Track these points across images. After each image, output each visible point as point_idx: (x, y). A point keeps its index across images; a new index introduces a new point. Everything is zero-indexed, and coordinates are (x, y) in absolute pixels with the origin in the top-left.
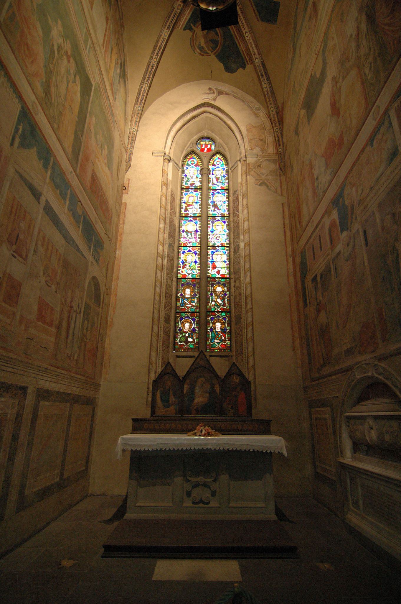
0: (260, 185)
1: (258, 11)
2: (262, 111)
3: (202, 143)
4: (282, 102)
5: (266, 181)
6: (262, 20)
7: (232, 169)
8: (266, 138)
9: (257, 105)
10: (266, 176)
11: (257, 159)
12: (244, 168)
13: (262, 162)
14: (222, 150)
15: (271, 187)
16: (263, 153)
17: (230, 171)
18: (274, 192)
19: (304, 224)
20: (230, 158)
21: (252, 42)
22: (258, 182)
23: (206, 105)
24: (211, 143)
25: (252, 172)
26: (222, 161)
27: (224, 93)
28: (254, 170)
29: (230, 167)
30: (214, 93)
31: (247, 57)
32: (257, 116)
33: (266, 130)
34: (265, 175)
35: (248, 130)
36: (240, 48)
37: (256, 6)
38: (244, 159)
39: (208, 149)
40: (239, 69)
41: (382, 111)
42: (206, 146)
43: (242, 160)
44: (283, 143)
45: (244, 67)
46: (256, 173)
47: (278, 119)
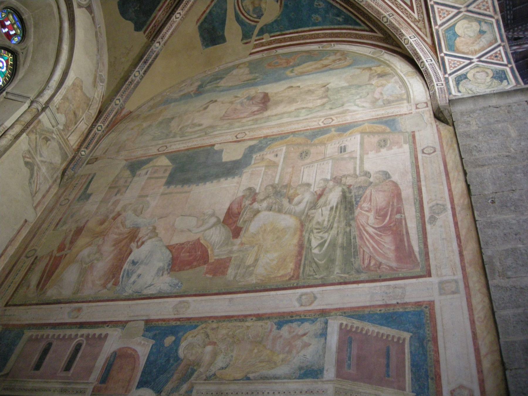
0: (27, 163)
1: (206, 18)
2: (103, 86)
3: (11, 17)
5: (36, 168)
6: (200, 27)
7: (9, 96)
9: (105, 74)
10: (42, 161)
11: (51, 128)
12: (28, 118)
13: (53, 138)
14: (21, 58)
15: (34, 182)
16: (62, 130)
17: (4, 93)
18: (32, 194)
19: (51, 293)
20: (20, 80)
21: (174, 26)
22: (28, 158)
24: (19, 31)
25: (33, 136)
26: (7, 70)
27: (93, 15)
28: (38, 136)
29: (9, 89)
31: (151, 27)
33: (88, 111)
34: (42, 159)
35: (74, 84)
36: (156, 11)
37: (210, 13)
38: (40, 108)
39: (8, 32)
40: (130, 22)
41: (316, 306)
42: (11, 27)
43: (35, 105)
45: (138, 28)
46: (36, 142)
47: (112, 119)
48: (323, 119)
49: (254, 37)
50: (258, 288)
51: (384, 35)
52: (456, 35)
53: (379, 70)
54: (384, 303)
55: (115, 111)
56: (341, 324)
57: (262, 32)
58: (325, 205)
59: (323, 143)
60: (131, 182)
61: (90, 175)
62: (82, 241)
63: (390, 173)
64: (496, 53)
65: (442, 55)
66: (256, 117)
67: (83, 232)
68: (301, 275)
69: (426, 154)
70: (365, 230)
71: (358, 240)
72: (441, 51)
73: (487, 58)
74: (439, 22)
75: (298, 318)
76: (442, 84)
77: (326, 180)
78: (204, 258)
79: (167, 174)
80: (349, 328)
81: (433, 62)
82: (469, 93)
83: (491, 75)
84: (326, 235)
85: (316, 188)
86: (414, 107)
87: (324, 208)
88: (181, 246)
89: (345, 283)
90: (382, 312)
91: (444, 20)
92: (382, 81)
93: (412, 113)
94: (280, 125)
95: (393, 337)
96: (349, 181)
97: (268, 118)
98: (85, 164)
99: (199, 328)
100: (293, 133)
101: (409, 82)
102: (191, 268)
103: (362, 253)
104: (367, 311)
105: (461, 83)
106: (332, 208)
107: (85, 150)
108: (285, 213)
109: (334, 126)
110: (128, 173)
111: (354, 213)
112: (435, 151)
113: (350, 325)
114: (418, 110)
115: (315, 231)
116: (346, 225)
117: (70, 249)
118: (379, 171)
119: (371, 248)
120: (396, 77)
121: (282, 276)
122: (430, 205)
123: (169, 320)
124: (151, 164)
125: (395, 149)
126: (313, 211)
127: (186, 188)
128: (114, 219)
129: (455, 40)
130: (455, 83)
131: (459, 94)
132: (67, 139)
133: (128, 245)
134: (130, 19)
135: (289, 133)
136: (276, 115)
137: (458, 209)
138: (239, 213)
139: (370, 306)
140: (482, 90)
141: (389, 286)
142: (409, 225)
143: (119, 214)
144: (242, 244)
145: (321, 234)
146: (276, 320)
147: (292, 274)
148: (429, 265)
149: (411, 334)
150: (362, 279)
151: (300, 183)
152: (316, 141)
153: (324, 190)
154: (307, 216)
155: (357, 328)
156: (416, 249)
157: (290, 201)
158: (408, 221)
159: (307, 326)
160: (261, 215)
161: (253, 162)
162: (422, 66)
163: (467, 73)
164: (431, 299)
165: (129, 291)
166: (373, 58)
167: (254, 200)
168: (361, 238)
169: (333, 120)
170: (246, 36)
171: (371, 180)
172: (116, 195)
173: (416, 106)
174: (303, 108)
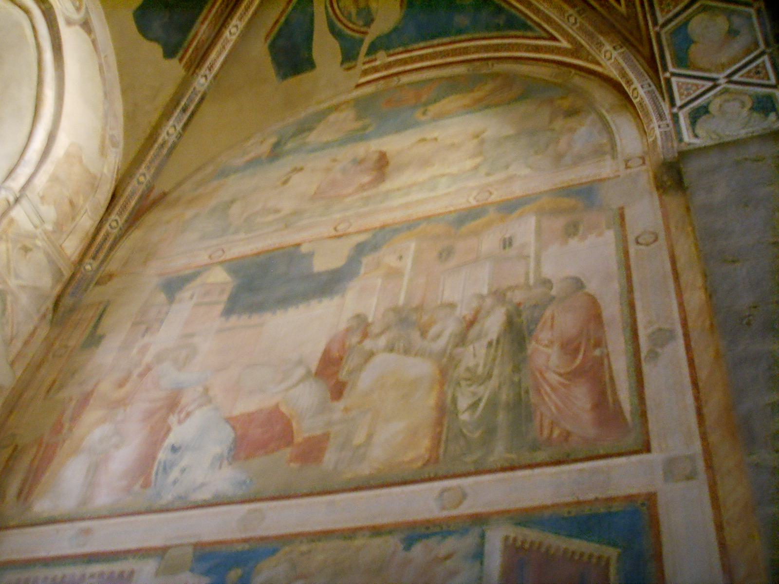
1: (281, 30)
4: (166, 190)
5: (9, 298)
8: (83, 212)
9: (119, 133)
19: (42, 506)
21: (228, 47)
23: (43, 7)
27: (93, 36)
28: (10, 245)
30: (78, 9)
31: (191, 50)
32: (103, 152)
34: (20, 282)
35: (68, 155)
37: (287, 22)
38: (12, 199)
41: (467, 508)
44: (103, 262)
45: (170, 52)
48: (474, 193)
49: (362, 58)
50: (372, 482)
51: (572, 44)
52: (689, 41)
53: (566, 104)
54: (576, 499)
55: (139, 192)
56: (506, 538)
57: (373, 49)
58: (479, 337)
59: (476, 233)
60: (167, 313)
61: (100, 303)
62: (91, 415)
63: (583, 279)
64: (757, 67)
65: (668, 75)
66: (365, 194)
67: (92, 401)
68: (441, 457)
69: (641, 244)
70: (544, 378)
71: (531, 393)
72: (665, 69)
73: (742, 76)
74: (661, 21)
75: (438, 529)
76: (668, 125)
77: (482, 297)
78: (286, 436)
79: (225, 297)
80: (519, 543)
81: (653, 87)
82: (711, 138)
83: (749, 105)
84: (481, 389)
85: (464, 311)
86: (623, 166)
87: (477, 345)
88: (249, 418)
89: (512, 468)
90: (573, 514)
91: (670, 15)
92: (572, 122)
93: (619, 176)
94: (406, 206)
95: (591, 556)
96: (518, 296)
97: (387, 195)
98: (91, 286)
99: (280, 554)
100: (428, 218)
101: (614, 122)
102: (266, 453)
103: (538, 418)
104: (547, 513)
105: (700, 121)
106: (490, 344)
107: (92, 261)
108: (416, 355)
109: (492, 203)
110: (162, 297)
111: (526, 349)
112: (656, 240)
113: (520, 538)
114: (629, 171)
115: (463, 383)
116: (513, 371)
117: (70, 430)
118: (567, 278)
119: (553, 408)
120: (593, 116)
121: (412, 461)
122: (650, 331)
123: (231, 542)
124: (198, 281)
125: (592, 238)
126: (460, 350)
127: (256, 319)
128: (142, 375)
129: (688, 48)
130: (688, 122)
131: (694, 141)
132: (61, 246)
133: (165, 419)
134: (156, 40)
135: (420, 219)
136: (399, 189)
137: (694, 335)
138: (341, 359)
139: (553, 506)
140: (735, 130)
141: (581, 471)
142: (615, 367)
143: (148, 369)
144: (346, 410)
145: (472, 389)
146: (403, 536)
147: (427, 457)
148: (647, 433)
149: (620, 550)
150: (539, 460)
151: (439, 302)
152: (464, 229)
153: (477, 312)
154: (451, 358)
155: (532, 543)
157: (423, 334)
158: (612, 358)
159: (450, 544)
160: (377, 360)
161: (362, 271)
162: (635, 95)
163: (709, 103)
164: (651, 489)
165: (168, 497)
166: (555, 84)
167: (365, 335)
168: (538, 391)
169: (491, 193)
170: (349, 56)
171: (553, 292)
172: (143, 336)
173: (626, 165)
174: (443, 175)
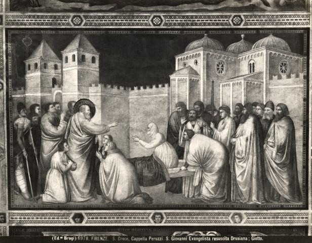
87: (241, 138)
156: (301, 187)
